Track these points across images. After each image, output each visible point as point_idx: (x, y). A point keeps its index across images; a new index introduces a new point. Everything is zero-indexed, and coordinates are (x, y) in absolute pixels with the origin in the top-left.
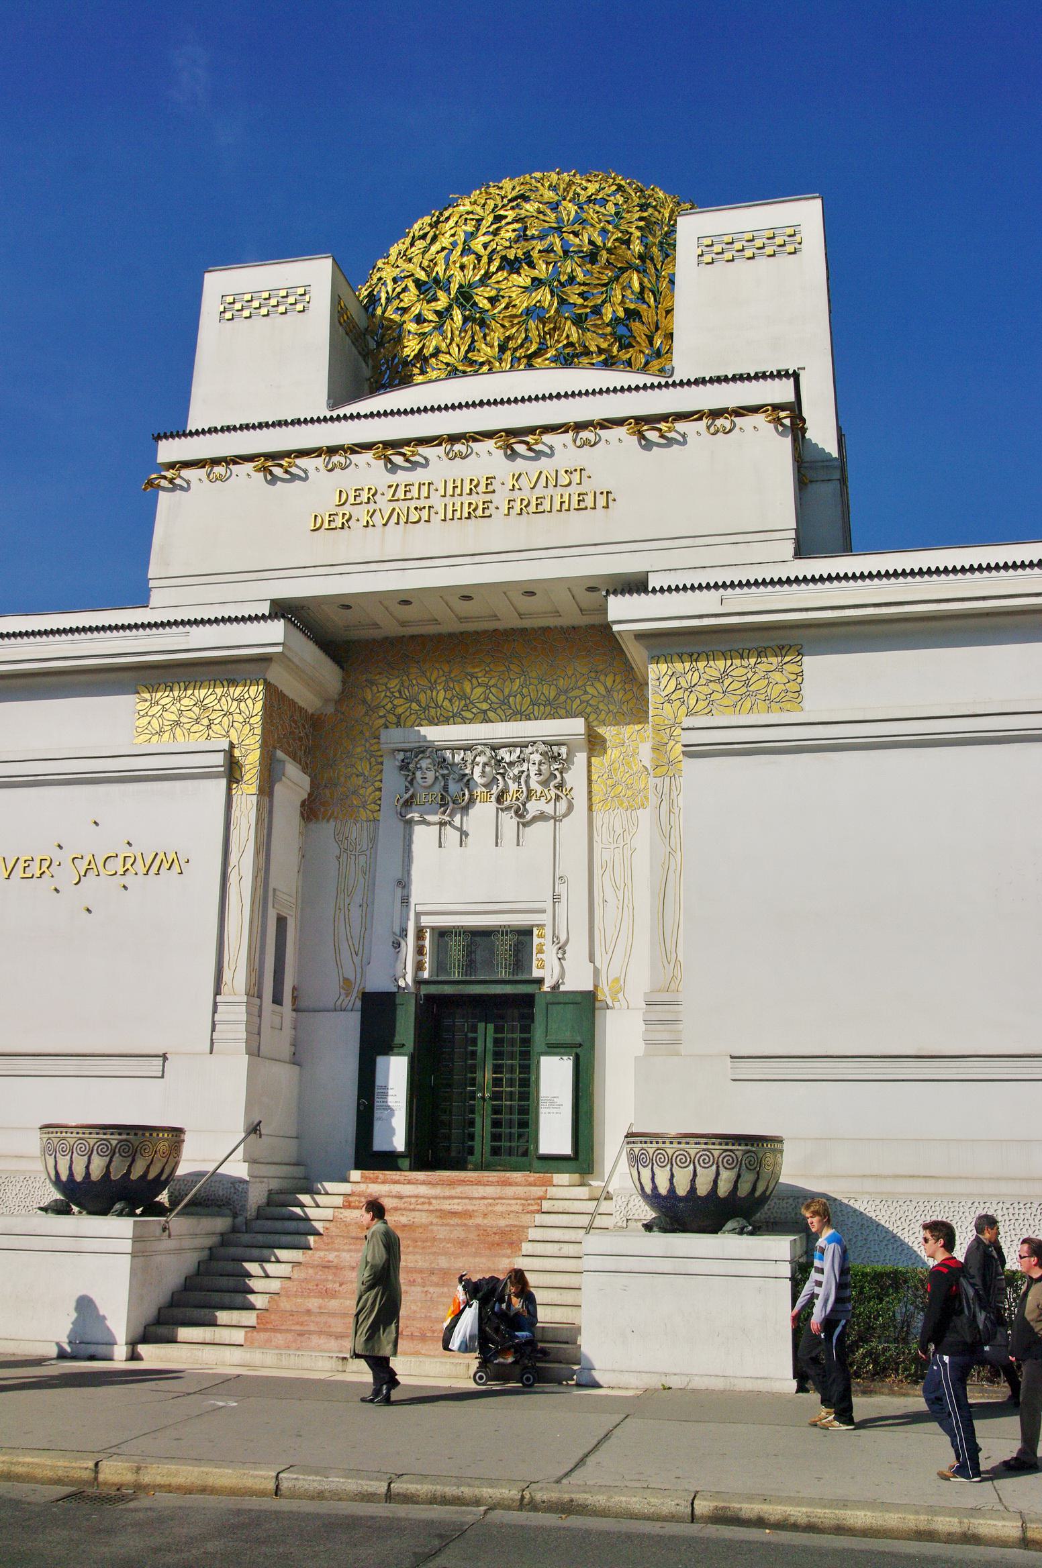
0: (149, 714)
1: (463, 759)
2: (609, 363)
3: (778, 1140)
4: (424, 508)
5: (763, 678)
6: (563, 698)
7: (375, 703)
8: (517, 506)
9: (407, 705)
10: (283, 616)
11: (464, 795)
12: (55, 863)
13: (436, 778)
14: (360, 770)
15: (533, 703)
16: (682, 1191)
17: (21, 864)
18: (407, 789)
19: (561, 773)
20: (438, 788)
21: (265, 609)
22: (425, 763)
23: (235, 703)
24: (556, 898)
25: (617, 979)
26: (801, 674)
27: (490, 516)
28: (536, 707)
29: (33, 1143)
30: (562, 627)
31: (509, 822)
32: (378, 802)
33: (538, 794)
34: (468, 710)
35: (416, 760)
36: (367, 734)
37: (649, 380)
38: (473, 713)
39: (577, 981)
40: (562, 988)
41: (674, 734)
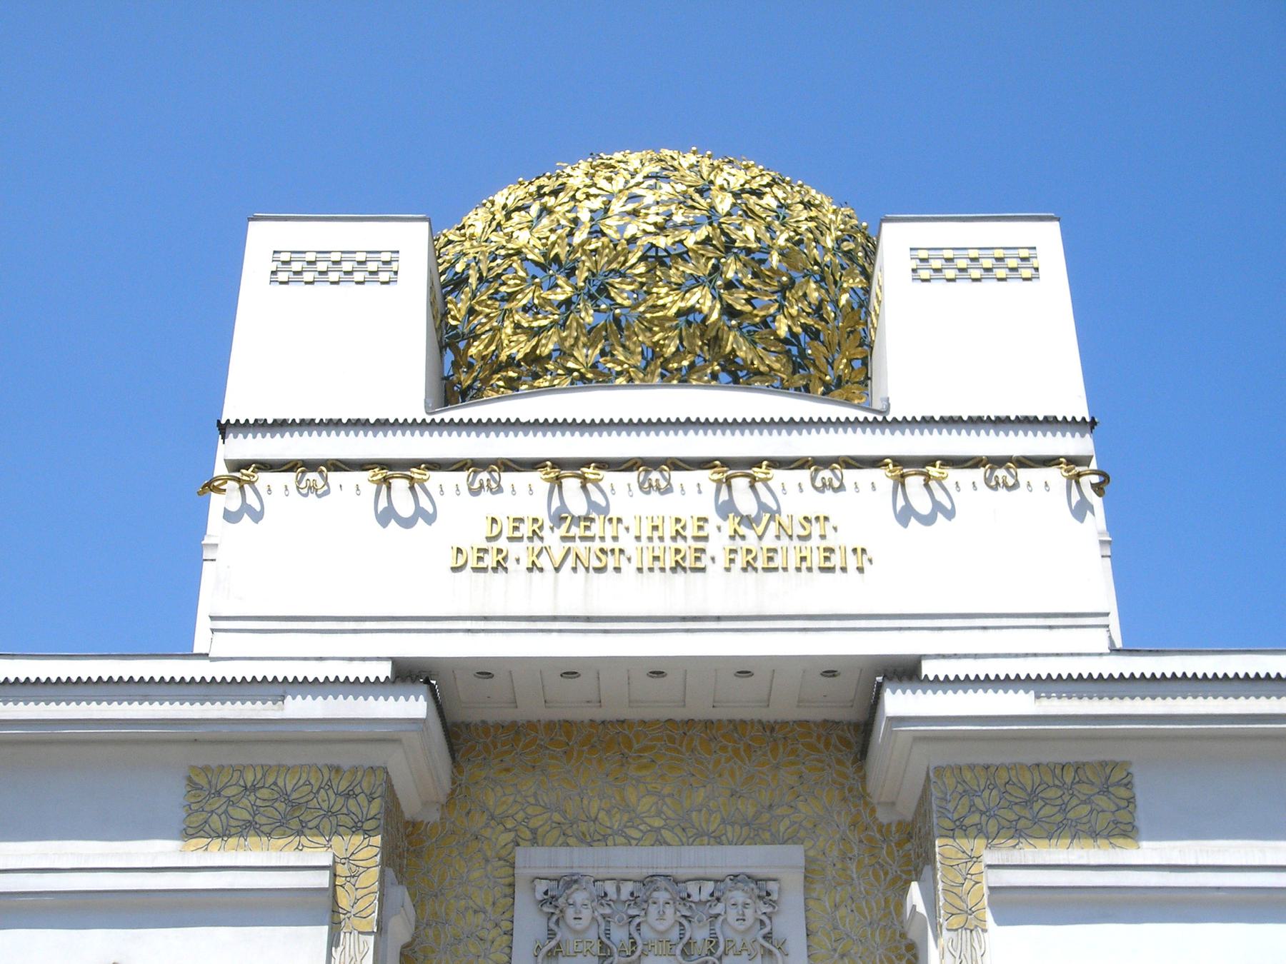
0: (208, 808)
1: (632, 894)
2: (783, 388)
4: (613, 551)
5: (1084, 802)
7: (497, 812)
8: (740, 560)
9: (546, 816)
10: (427, 682)
11: (634, 944)
13: (594, 919)
14: (479, 903)
15: (723, 821)
18: (551, 934)
19: (770, 918)
20: (592, 935)
21: (384, 671)
22: (579, 897)
23: (341, 800)
26: (1132, 800)
27: (703, 570)
28: (729, 828)
30: (760, 722)
32: (507, 950)
34: (628, 827)
35: (568, 892)
36: (489, 854)
37: (852, 413)
38: (641, 831)
41: (971, 872)
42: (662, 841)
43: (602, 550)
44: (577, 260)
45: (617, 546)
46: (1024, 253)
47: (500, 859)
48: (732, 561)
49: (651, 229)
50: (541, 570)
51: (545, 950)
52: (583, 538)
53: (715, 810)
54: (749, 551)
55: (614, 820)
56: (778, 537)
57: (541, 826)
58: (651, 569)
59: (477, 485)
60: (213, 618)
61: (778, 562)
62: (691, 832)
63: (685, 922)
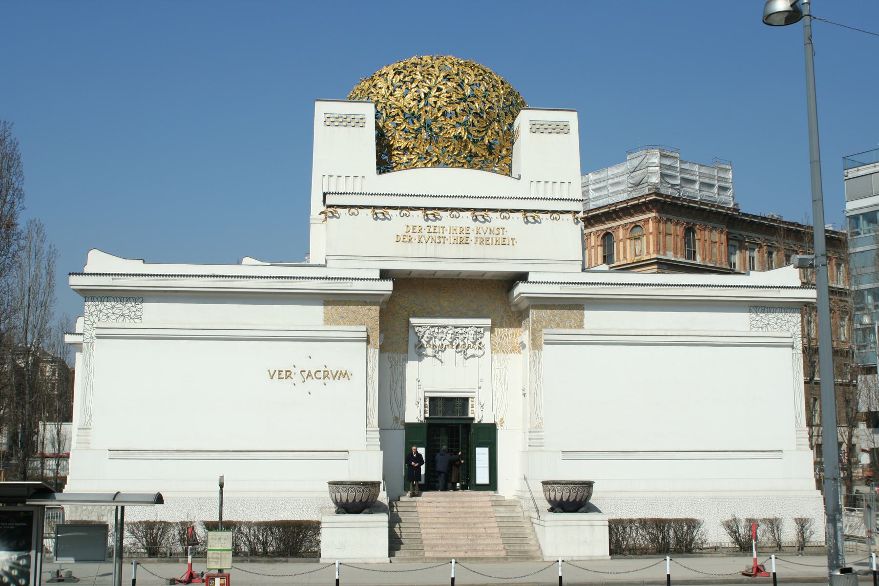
3: (593, 482)
10: (393, 280)
11: (442, 345)
12: (293, 374)
16: (564, 500)
17: (277, 373)
24: (480, 387)
25: (502, 419)
29: (327, 487)
30: (479, 280)
31: (460, 357)
33: (472, 346)
39: (487, 420)
40: (482, 422)
44: (421, 114)
45: (444, 235)
46: (565, 124)
47: (404, 319)
49: (445, 104)
51: (418, 347)
59: (402, 215)
61: (490, 242)
63: (457, 339)
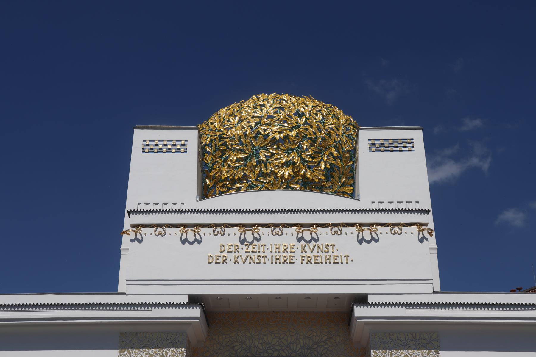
4: (263, 256)
6: (316, 346)
9: (241, 345)
10: (200, 304)
27: (293, 263)
34: (269, 349)
42: (280, 354)
43: (259, 256)
45: (264, 254)
48: (303, 260)
50: (238, 263)
52: (253, 252)
53: (298, 343)
54: (309, 257)
55: (263, 347)
56: (318, 252)
57: (238, 349)
58: (276, 263)
60: (127, 280)
61: (319, 260)
62: (290, 351)
